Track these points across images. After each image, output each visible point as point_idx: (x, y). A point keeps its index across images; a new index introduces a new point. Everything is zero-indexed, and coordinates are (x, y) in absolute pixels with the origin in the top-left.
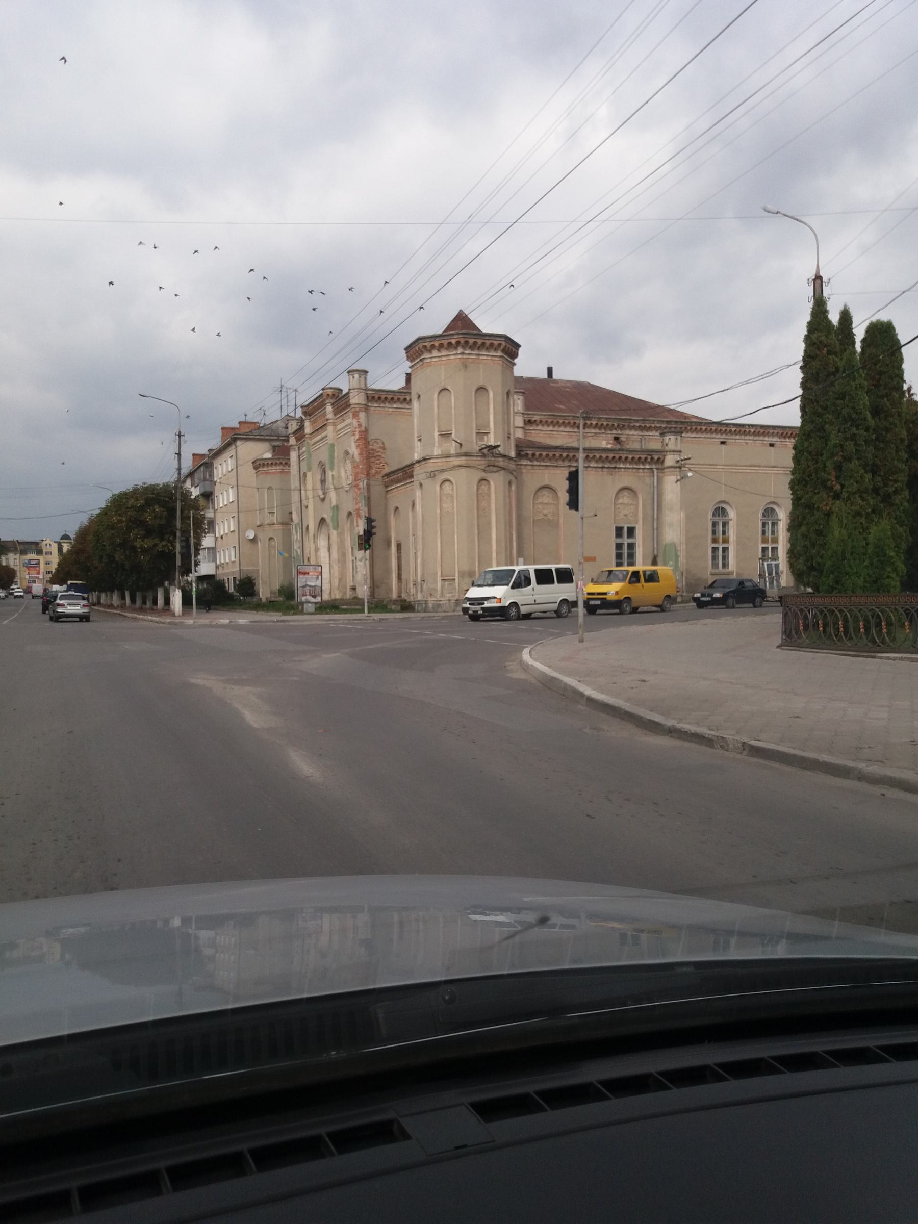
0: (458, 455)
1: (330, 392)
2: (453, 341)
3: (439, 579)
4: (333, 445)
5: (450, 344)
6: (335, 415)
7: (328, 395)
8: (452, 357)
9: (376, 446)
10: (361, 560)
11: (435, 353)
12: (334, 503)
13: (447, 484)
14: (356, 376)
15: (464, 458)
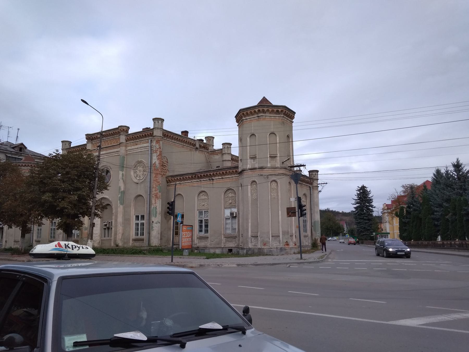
0: (281, 168)
1: (125, 128)
2: (280, 110)
3: (271, 235)
4: (124, 157)
5: (278, 111)
6: (127, 141)
7: (124, 130)
8: (277, 118)
9: (164, 160)
10: (156, 223)
11: (267, 114)
12: (122, 189)
13: (274, 183)
14: (160, 122)
15: (284, 170)
